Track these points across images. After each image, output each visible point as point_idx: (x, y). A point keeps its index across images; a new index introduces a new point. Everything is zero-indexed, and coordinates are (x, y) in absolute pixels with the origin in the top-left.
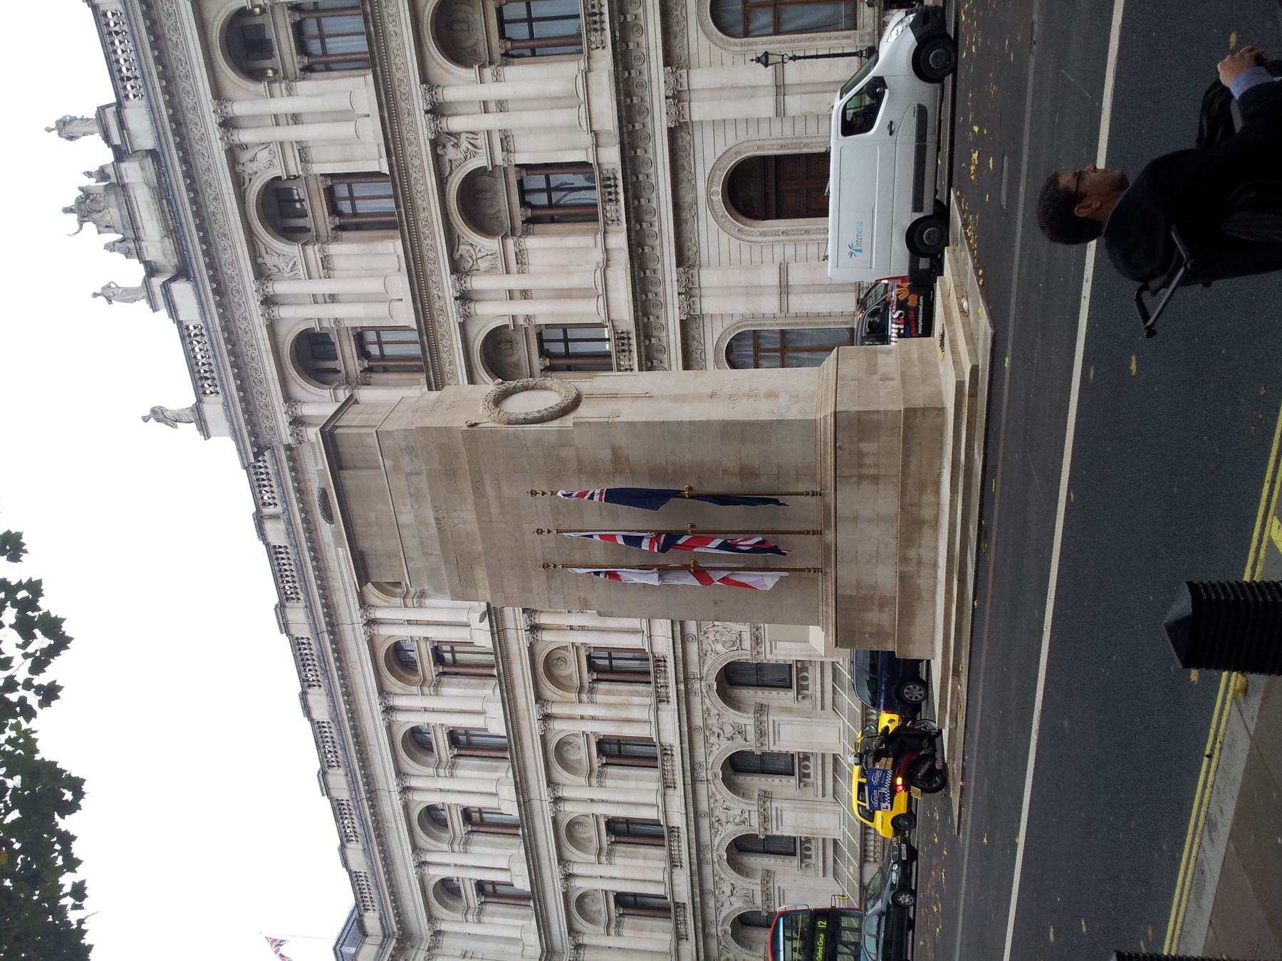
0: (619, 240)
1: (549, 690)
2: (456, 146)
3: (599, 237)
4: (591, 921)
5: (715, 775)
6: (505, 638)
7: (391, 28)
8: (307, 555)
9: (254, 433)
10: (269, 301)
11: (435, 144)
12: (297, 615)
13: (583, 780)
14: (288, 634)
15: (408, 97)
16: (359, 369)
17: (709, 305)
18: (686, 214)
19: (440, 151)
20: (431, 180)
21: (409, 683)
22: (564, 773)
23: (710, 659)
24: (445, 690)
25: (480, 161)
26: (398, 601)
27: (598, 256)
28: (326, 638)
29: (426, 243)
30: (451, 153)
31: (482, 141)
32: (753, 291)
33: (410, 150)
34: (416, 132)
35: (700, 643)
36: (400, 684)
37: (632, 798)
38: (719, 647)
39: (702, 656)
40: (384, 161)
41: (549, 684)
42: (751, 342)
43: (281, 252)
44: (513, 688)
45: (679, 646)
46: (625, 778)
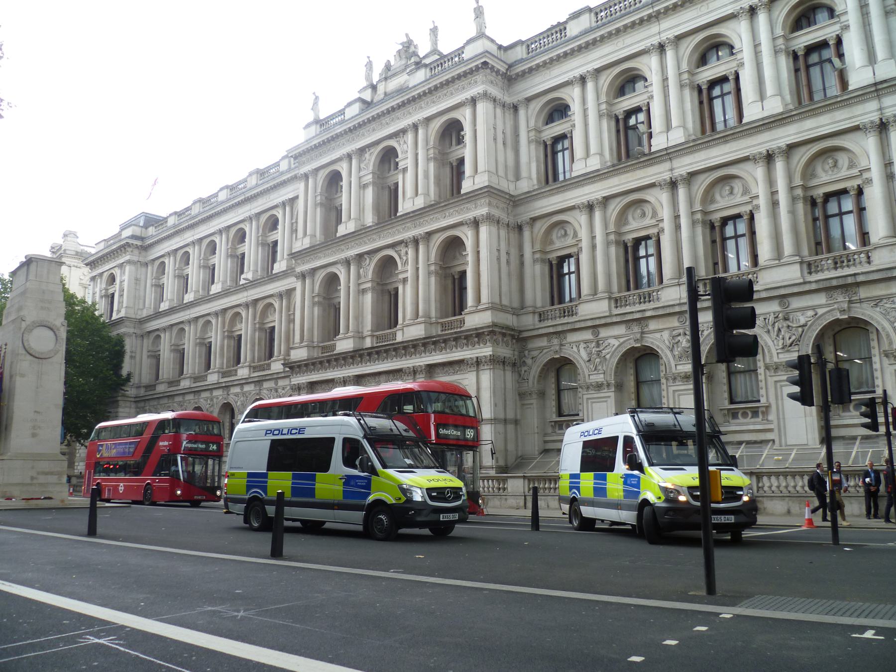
4: (153, 343)
8: (271, 184)
20: (390, 241)
38: (239, 403)
46: (200, 357)
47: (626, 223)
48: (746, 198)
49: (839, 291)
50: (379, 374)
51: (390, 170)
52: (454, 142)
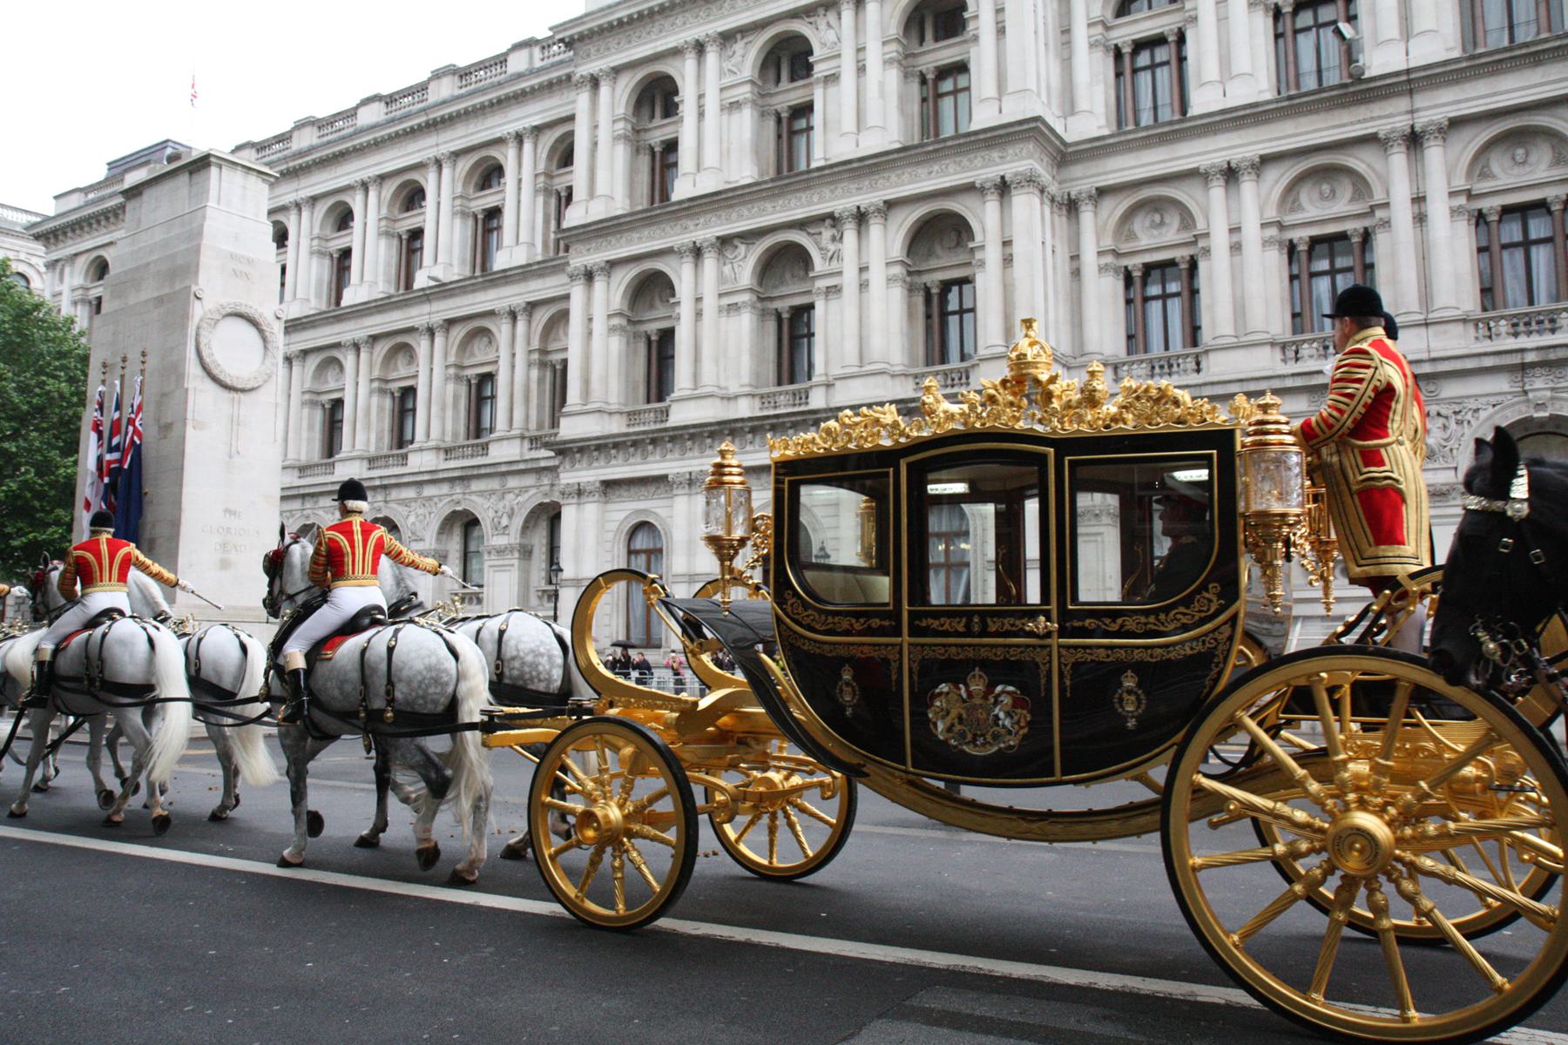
0: (745, 409)
1: (382, 348)
2: (834, 239)
3: (747, 390)
5: (308, 517)
6: (422, 303)
7: (936, 168)
8: (493, 95)
9: (582, 38)
10: (700, 48)
11: (832, 219)
12: (445, 89)
13: (307, 386)
14: (430, 80)
15: (873, 189)
16: (652, 142)
19: (828, 222)
20: (799, 214)
21: (391, 205)
22: (313, 367)
23: (402, 510)
24: (383, 242)
25: (819, 265)
26: (459, 190)
27: (734, 389)
28: (422, 119)
29: (744, 211)
31: (835, 266)
33: (826, 191)
34: (842, 197)
35: (415, 500)
36: (389, 196)
37: (291, 435)
38: (412, 519)
39: (404, 502)
40: (822, 163)
41: (387, 348)
43: (748, 56)
44: (380, 312)
45: (411, 479)
46: (311, 427)
47: (1296, 207)
48: (1186, 236)
49: (1538, 371)
51: (778, 80)
52: (929, 34)
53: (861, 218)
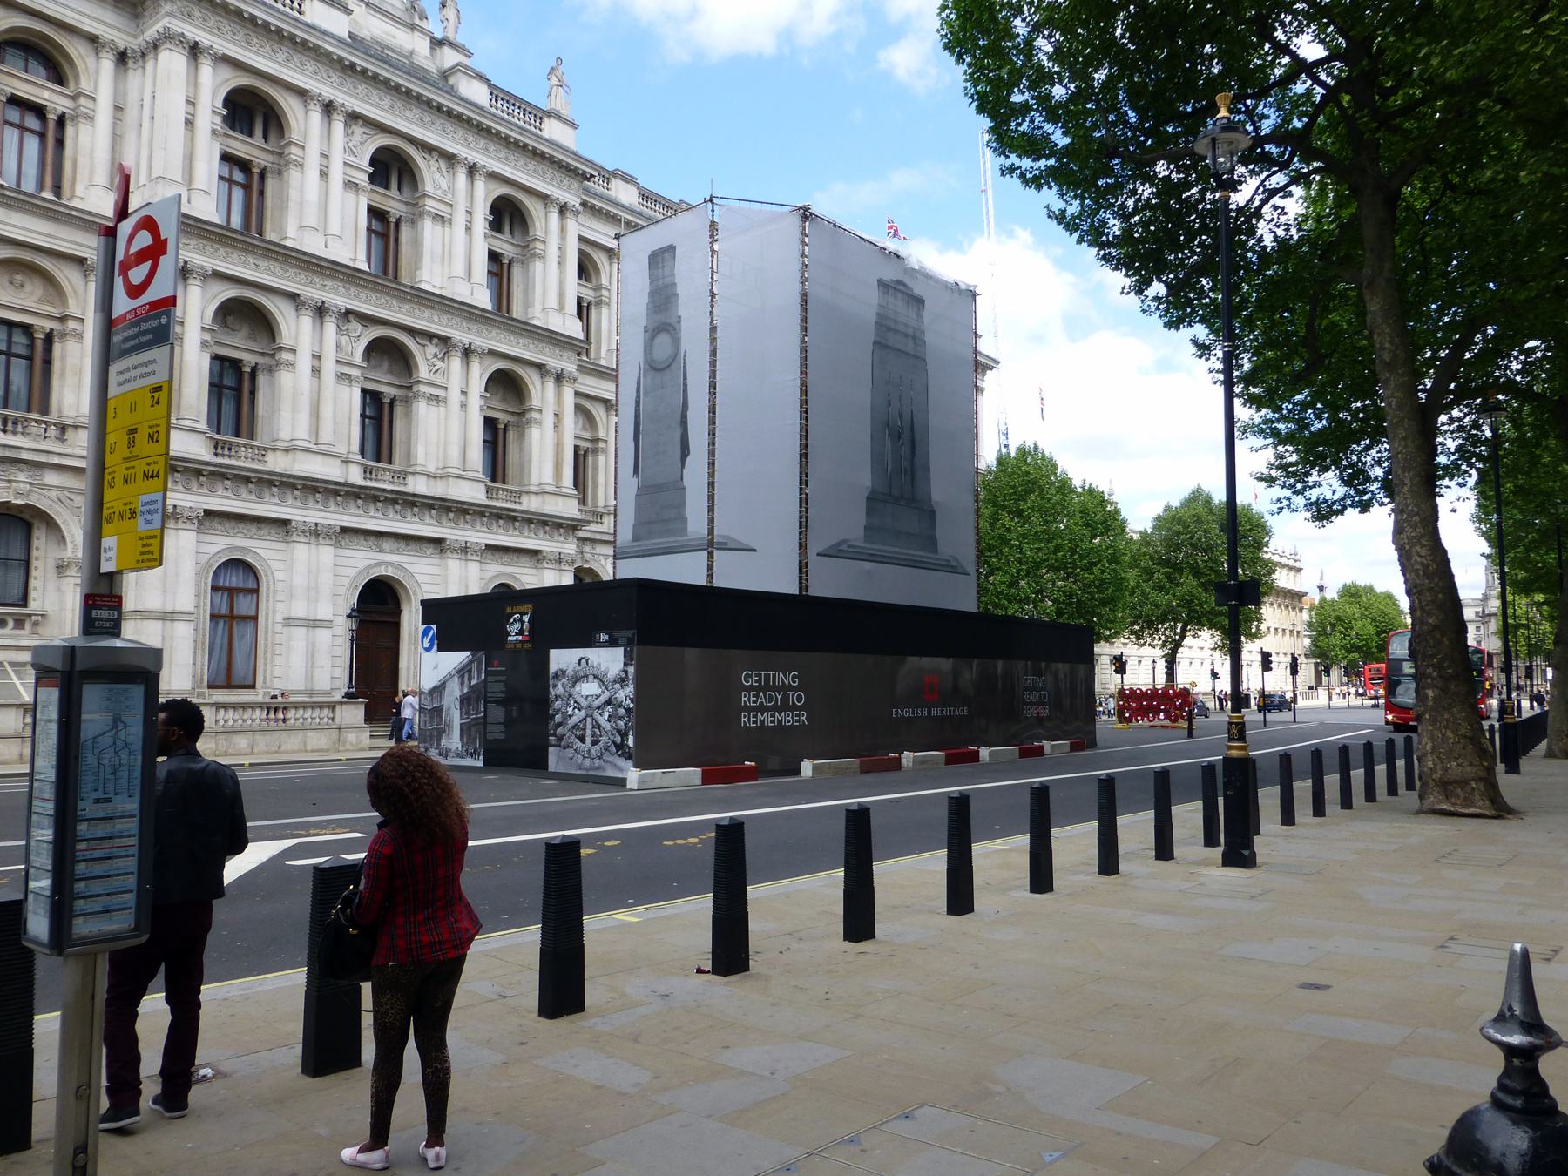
2: (436, 355)
11: (444, 340)
17: (302, 551)
18: (372, 541)
20: (420, 324)
25: (423, 371)
30: (431, 349)
31: (438, 379)
32: (312, 593)
42: (241, 585)
50: (380, 535)
53: (467, 352)
